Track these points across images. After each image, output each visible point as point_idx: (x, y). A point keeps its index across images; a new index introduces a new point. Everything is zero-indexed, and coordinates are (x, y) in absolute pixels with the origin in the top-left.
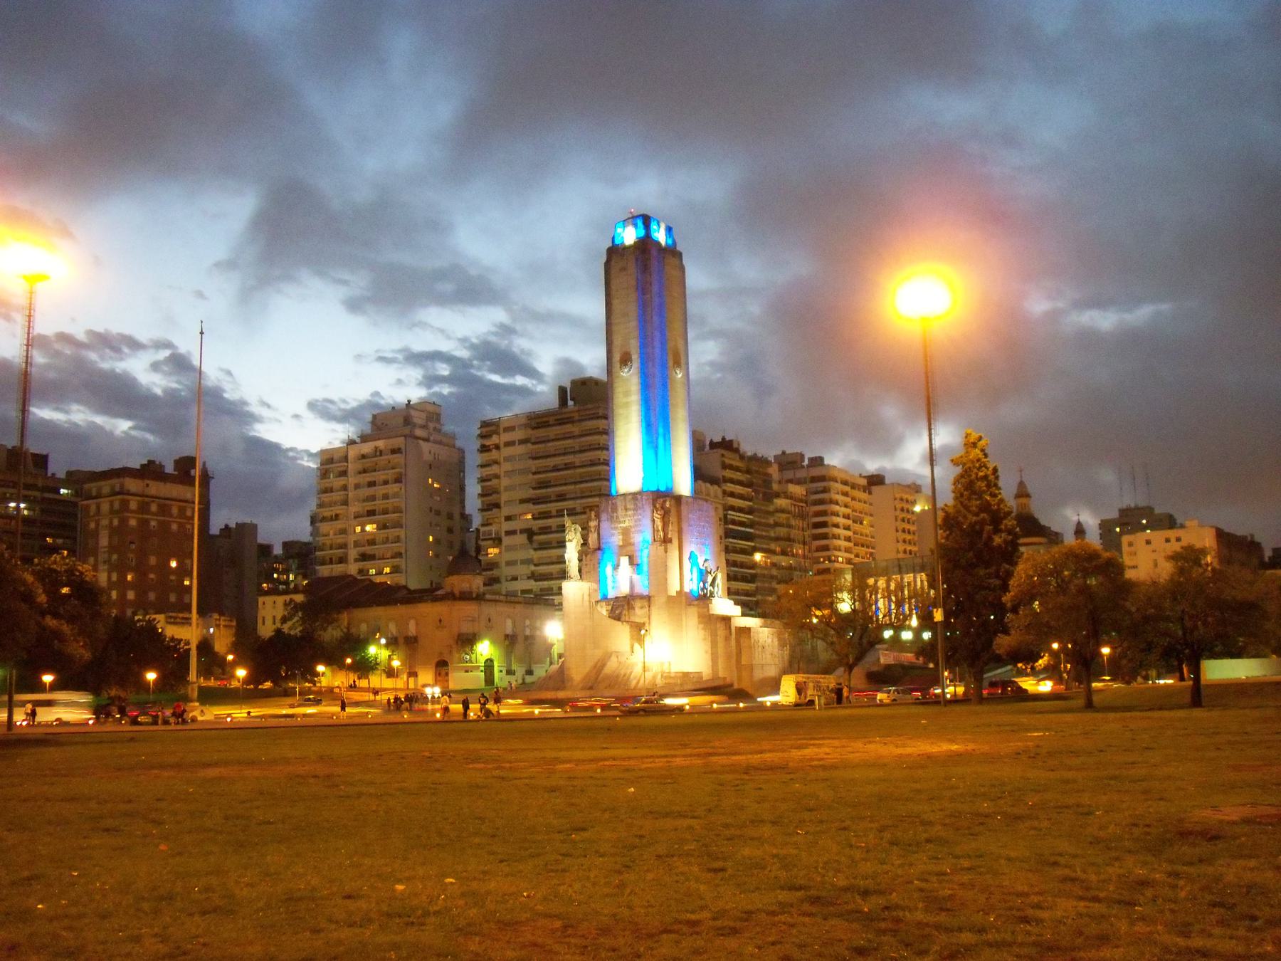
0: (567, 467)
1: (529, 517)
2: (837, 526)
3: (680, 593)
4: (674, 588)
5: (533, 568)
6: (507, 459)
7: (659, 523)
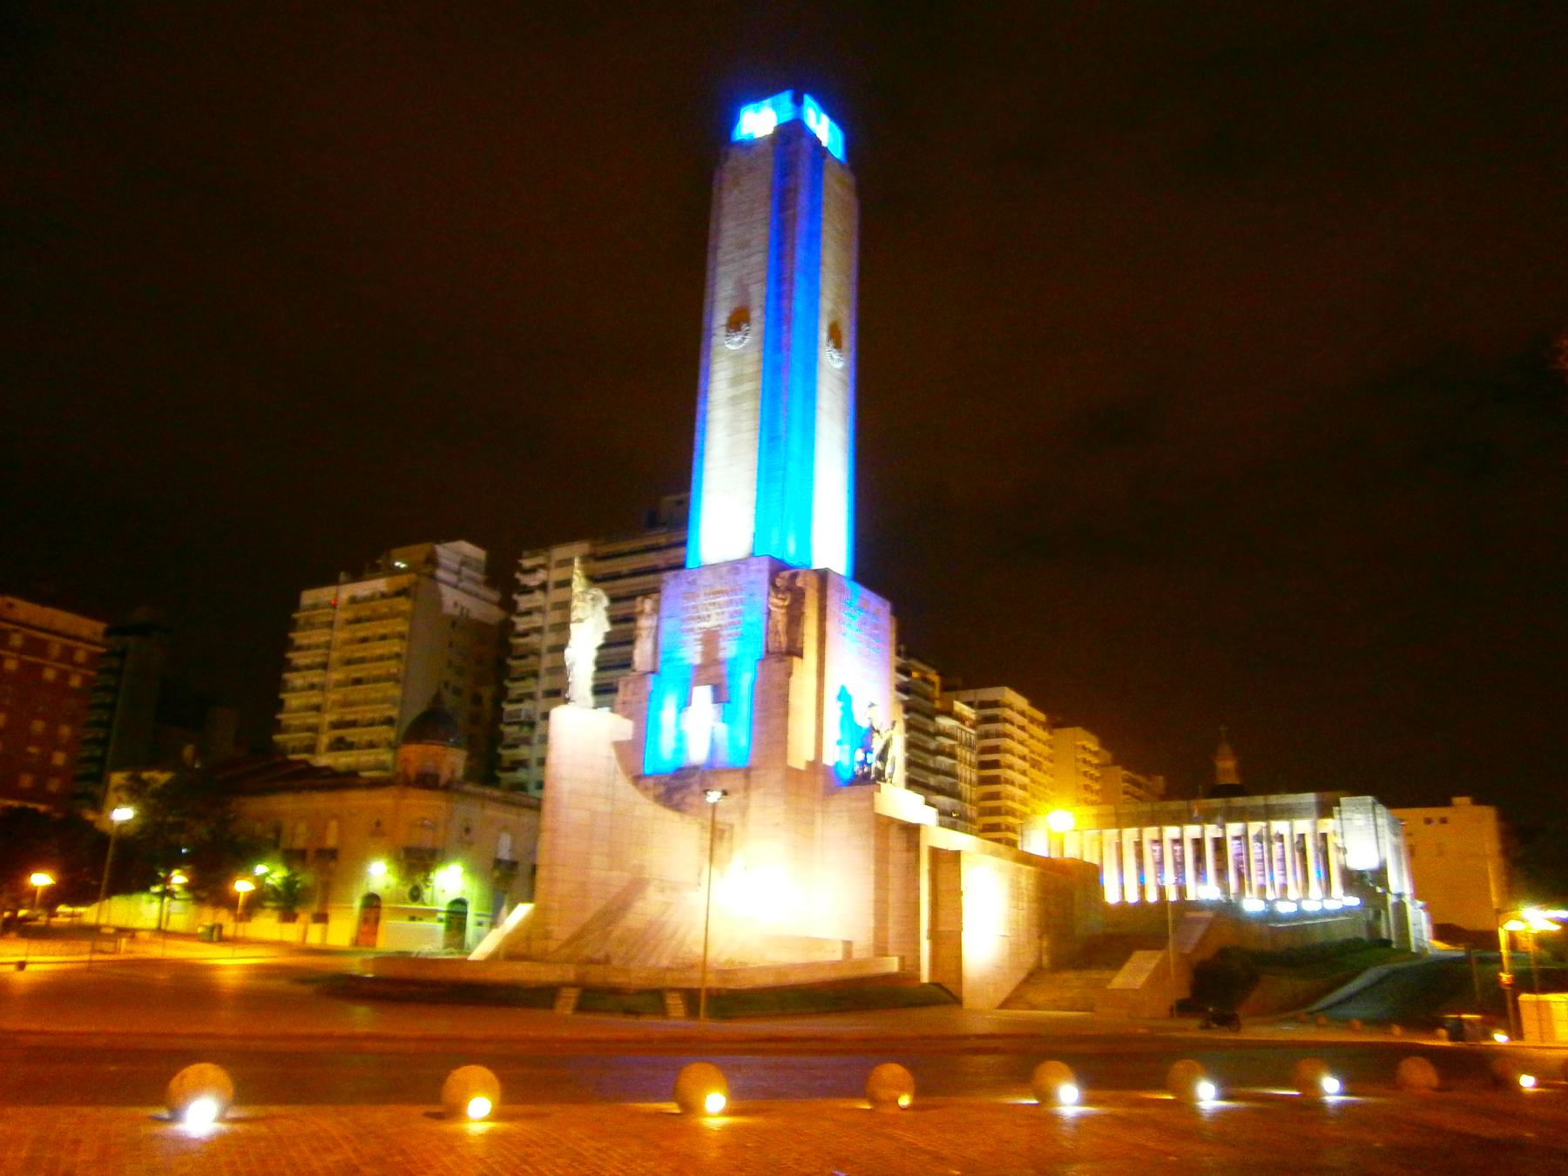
2: (1010, 767)
3: (815, 766)
4: (801, 752)
7: (780, 616)
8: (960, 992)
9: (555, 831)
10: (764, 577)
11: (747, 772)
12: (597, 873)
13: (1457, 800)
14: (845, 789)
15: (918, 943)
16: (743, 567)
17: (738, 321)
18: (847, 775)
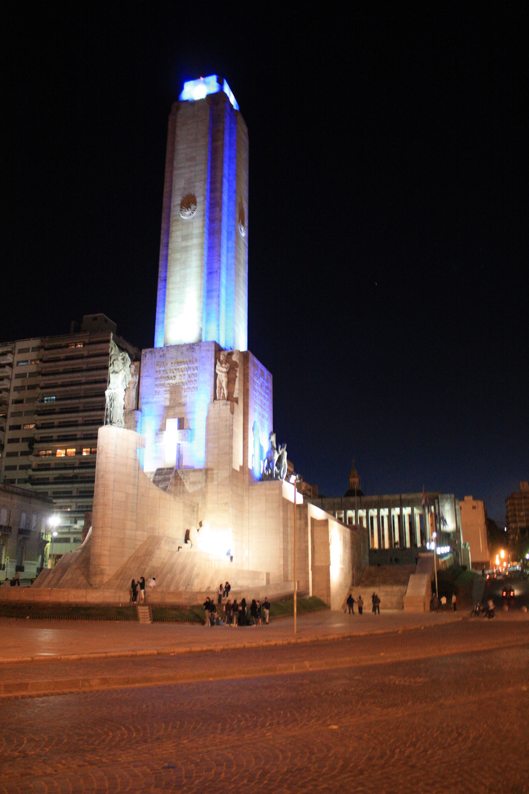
0: (72, 384)
1: (32, 426)
3: (244, 467)
5: (30, 472)
6: (18, 376)
7: (223, 378)
8: (329, 601)
9: (105, 505)
10: (212, 354)
11: (206, 471)
12: (128, 532)
13: (466, 498)
14: (260, 483)
15: (308, 574)
16: (197, 348)
17: (188, 202)
18: (257, 474)
